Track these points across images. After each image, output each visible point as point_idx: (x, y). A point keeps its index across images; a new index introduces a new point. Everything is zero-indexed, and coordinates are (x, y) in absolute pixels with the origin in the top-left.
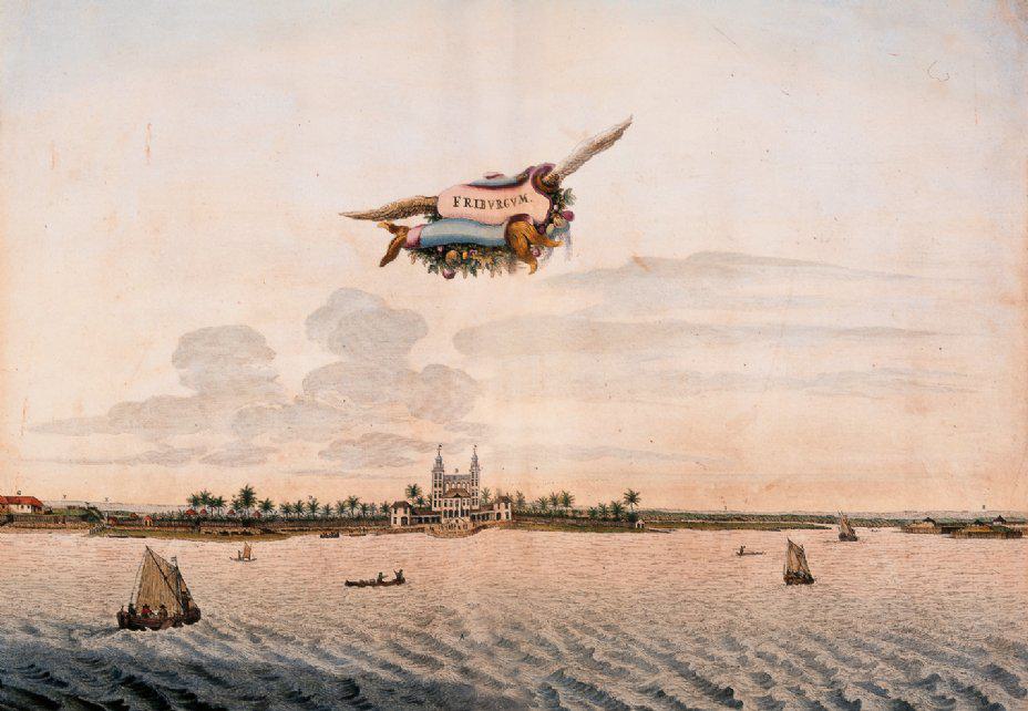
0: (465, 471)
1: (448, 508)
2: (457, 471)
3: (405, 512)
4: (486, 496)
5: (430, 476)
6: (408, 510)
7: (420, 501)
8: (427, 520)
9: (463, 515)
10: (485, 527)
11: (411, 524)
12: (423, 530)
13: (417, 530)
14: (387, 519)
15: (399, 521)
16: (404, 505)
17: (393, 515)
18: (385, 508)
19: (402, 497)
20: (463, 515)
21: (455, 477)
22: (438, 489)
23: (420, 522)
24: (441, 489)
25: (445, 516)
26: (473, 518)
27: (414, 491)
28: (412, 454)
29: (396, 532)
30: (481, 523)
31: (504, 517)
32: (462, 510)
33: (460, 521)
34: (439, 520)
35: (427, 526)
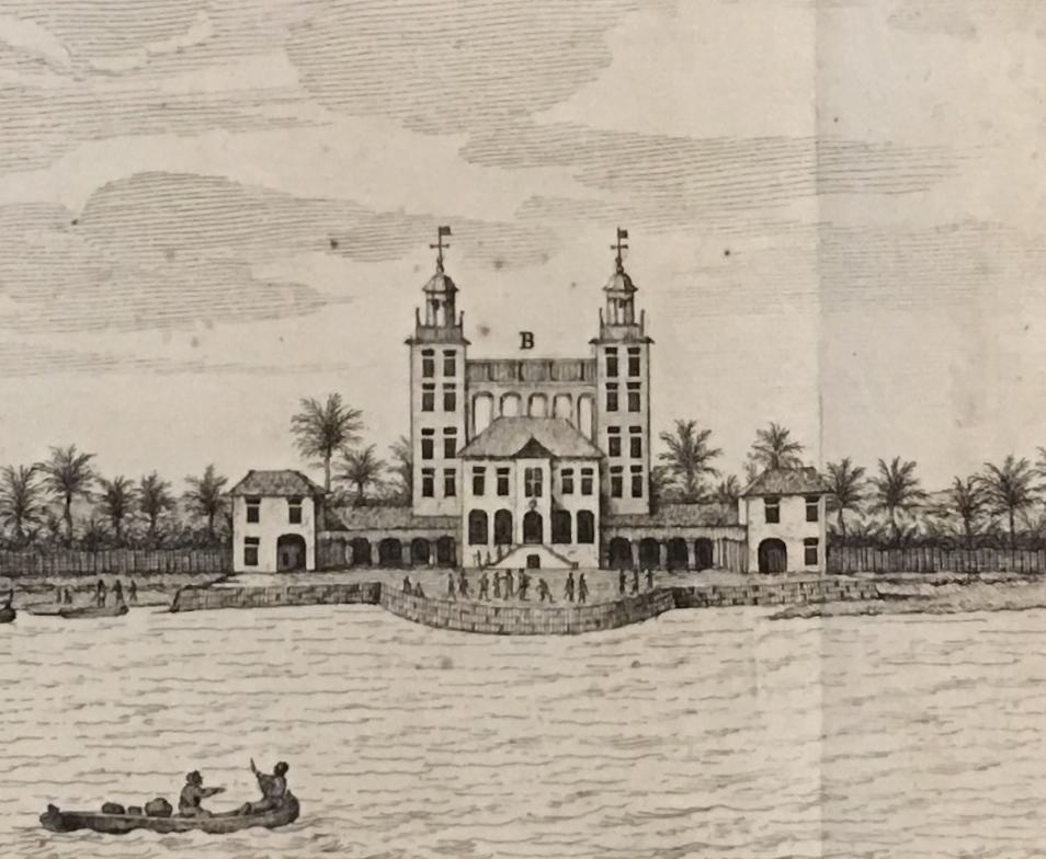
0: (570, 340)
1: (491, 503)
2: (528, 340)
3: (295, 517)
4: (690, 455)
5: (402, 365)
6: (308, 506)
7: (362, 471)
8: (391, 554)
9: (561, 535)
10: (683, 599)
11: (321, 568)
12: (375, 595)
13: (351, 595)
14: (215, 543)
15: (268, 555)
16: (295, 490)
17: (242, 528)
18: (209, 498)
19: (287, 455)
20: (561, 535)
21: (516, 367)
22: (438, 419)
23: (361, 555)
24: (456, 419)
25: (478, 536)
26: (615, 554)
27: (329, 431)
28: (327, 271)
29: (252, 600)
30: (666, 580)
31: (796, 554)
32: (560, 516)
33: (547, 561)
34: (446, 553)
35: (392, 579)
